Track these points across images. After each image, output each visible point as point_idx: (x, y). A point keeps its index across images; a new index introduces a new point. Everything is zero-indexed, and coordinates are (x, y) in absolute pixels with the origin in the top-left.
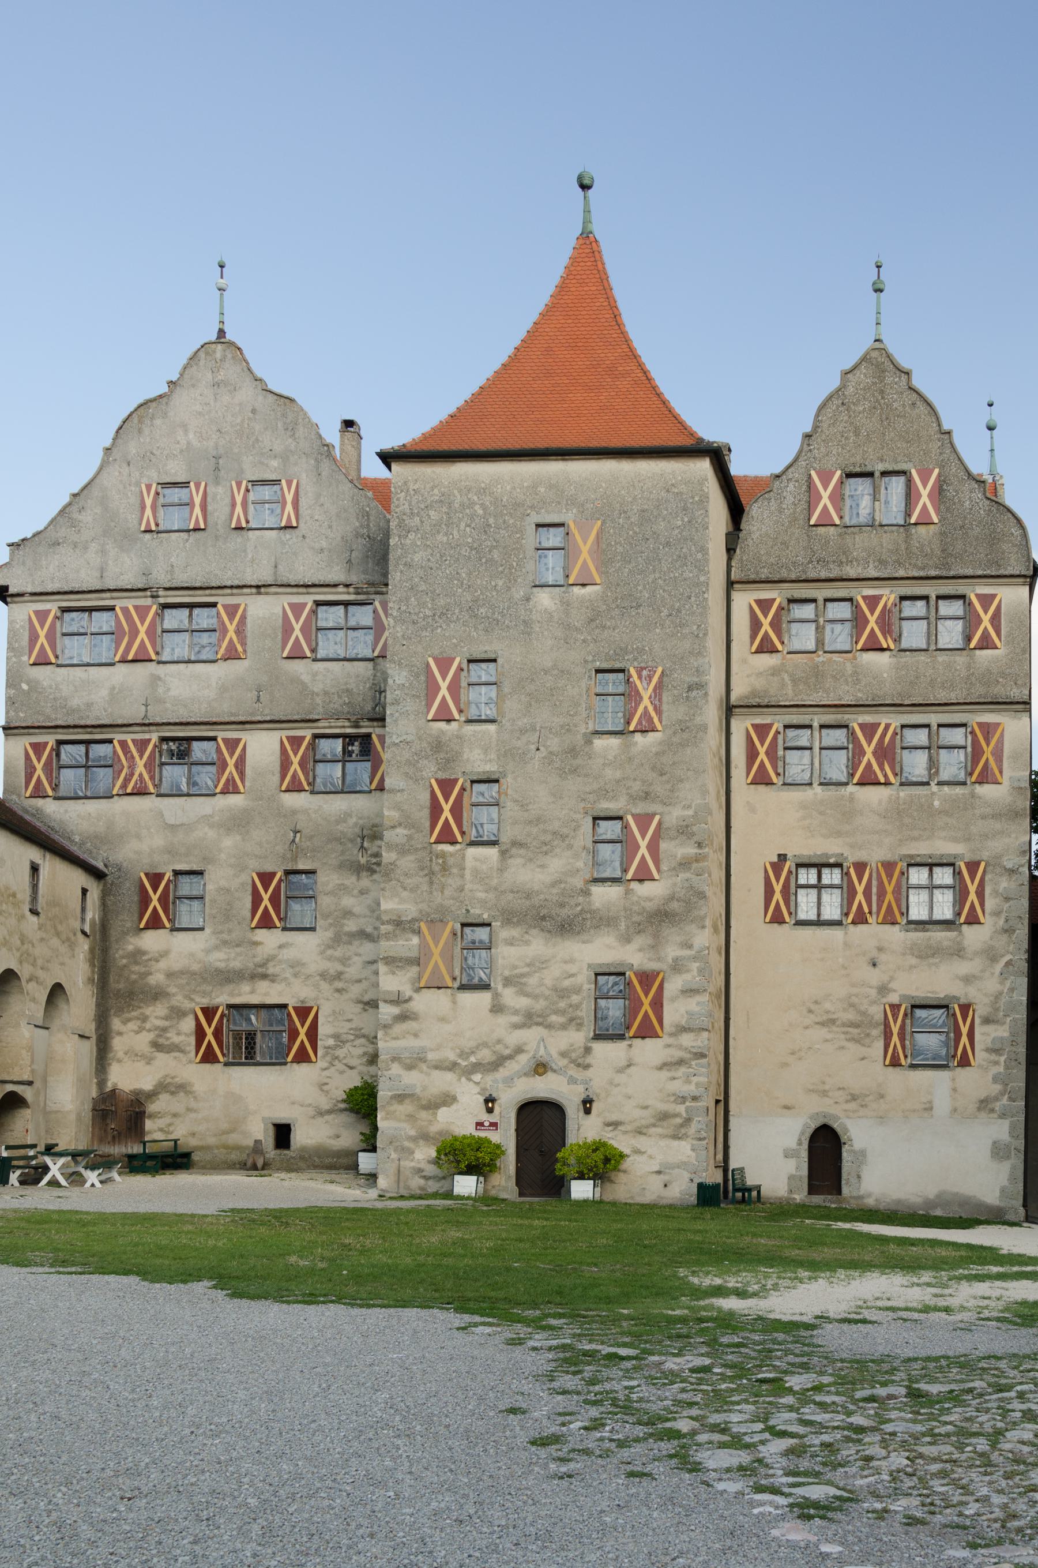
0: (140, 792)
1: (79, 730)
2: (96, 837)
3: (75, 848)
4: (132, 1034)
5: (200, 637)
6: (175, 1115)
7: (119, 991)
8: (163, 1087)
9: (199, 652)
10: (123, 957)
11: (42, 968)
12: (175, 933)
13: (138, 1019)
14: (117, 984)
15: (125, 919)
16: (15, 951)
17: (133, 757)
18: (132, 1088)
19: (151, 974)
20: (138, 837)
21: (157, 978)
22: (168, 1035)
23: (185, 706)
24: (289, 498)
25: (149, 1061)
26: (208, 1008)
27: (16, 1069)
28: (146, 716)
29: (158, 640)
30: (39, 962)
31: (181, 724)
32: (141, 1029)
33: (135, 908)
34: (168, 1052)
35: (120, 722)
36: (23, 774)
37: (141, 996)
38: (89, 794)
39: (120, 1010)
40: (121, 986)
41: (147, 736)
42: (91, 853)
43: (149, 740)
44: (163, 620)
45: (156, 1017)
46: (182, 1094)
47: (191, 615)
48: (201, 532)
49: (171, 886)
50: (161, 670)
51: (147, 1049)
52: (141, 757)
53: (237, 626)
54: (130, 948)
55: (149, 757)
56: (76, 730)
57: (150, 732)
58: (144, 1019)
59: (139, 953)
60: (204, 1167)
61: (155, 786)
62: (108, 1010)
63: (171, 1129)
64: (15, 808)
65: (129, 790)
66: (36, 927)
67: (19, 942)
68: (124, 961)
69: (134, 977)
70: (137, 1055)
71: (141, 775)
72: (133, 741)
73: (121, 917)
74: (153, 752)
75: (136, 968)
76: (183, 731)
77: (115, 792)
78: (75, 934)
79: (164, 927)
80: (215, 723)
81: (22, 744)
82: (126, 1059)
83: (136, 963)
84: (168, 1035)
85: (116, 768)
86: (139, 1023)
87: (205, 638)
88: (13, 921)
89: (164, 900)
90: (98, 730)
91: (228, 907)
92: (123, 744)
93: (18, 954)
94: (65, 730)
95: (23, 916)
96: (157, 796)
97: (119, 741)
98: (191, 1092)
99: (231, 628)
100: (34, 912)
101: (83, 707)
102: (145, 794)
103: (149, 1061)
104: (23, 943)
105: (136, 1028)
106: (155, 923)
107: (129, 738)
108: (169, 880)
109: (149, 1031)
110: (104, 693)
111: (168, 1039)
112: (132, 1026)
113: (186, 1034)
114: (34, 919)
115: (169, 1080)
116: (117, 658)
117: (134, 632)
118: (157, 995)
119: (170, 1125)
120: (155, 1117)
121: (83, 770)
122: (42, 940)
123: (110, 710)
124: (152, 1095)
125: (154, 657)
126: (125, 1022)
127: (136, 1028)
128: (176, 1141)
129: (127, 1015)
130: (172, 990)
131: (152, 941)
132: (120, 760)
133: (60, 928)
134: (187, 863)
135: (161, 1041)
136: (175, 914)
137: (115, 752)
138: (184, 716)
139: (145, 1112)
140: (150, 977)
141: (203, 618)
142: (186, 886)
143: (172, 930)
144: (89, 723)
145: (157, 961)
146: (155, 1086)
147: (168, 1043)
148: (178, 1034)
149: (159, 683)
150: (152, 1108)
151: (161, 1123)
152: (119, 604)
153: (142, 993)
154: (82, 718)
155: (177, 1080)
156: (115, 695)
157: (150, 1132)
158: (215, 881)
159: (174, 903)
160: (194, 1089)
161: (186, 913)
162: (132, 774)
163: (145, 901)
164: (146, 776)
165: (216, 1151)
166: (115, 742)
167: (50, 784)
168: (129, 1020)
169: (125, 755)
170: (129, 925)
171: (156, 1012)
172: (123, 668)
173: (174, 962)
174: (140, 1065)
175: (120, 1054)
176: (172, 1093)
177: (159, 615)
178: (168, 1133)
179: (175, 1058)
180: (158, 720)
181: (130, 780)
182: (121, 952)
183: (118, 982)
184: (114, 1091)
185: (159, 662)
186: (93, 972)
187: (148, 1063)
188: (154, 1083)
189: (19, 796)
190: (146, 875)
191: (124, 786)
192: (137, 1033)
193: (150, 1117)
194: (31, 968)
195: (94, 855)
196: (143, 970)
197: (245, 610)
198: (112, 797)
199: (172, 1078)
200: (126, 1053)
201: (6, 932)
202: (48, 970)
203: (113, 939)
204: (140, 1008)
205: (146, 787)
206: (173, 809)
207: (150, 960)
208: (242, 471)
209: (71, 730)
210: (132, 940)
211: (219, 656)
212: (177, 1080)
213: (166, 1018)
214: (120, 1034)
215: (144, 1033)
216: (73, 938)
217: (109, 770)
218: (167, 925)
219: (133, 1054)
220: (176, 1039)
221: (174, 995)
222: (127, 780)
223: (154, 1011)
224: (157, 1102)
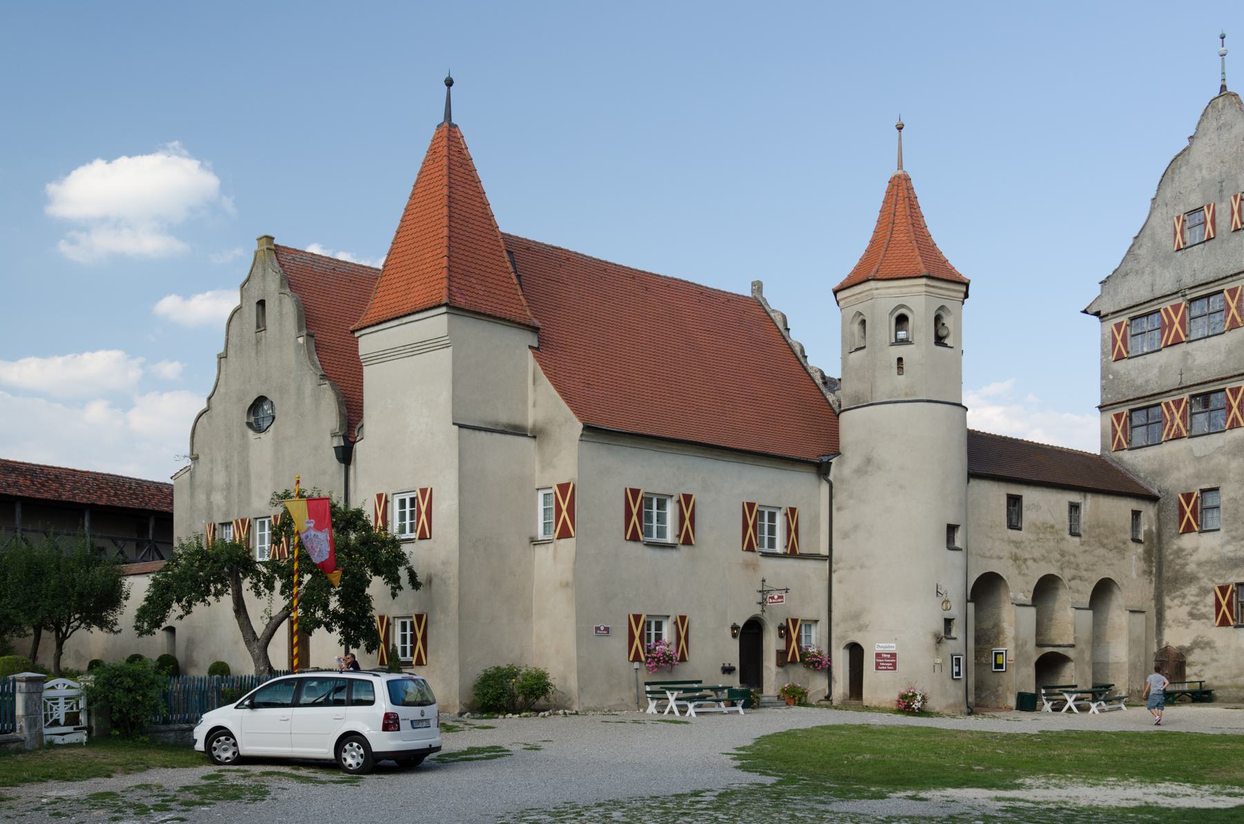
0: (1178, 437)
1: (1142, 400)
2: (1153, 472)
3: (1141, 482)
4: (1177, 607)
5: (1214, 317)
6: (1204, 664)
7: (1169, 578)
8: (1197, 644)
9: (1214, 328)
10: (1171, 554)
11: (1086, 570)
12: (1202, 534)
13: (1180, 596)
14: (1168, 574)
15: (1172, 527)
16: (1054, 563)
17: (1173, 413)
18: (1177, 645)
19: (1187, 564)
20: (1178, 469)
21: (1191, 568)
22: (1199, 607)
23: (1205, 370)
24: (1209, 218)
25: (1187, 626)
26: (1222, 587)
27: (1066, 637)
28: (1181, 382)
29: (1187, 325)
30: (1083, 566)
31: (1201, 384)
32: (1182, 604)
33: (1177, 519)
34: (1199, 619)
35: (1165, 390)
36: (1111, 436)
37: (1182, 581)
38: (1149, 443)
39: (1170, 591)
40: (1170, 574)
41: (1182, 396)
42: (1151, 484)
43: (1183, 399)
44: (1190, 311)
45: (1192, 595)
46: (1208, 649)
47: (1209, 302)
48: (1212, 240)
49: (1199, 501)
50: (1189, 347)
51: (1186, 618)
52: (1178, 412)
53: (1237, 303)
54: (1175, 547)
55: (1183, 411)
56: (1139, 401)
57: (1183, 393)
58: (1184, 597)
59: (1181, 550)
60: (1223, 701)
61: (1187, 431)
62: (1163, 592)
63: (1202, 673)
64: (1107, 459)
65: (1171, 437)
66: (1079, 543)
67: (1059, 557)
68: (1172, 557)
69: (1177, 567)
70: (1180, 622)
71: (1178, 425)
72: (1173, 401)
73: (1169, 527)
74: (1186, 406)
75: (1178, 561)
76: (1203, 388)
77: (1163, 440)
78: (1125, 543)
79: (1195, 531)
80: (1222, 379)
81: (1110, 415)
82: (1173, 625)
83: (1179, 558)
84: (1199, 607)
85: (1164, 422)
86: (1181, 600)
87: (1218, 317)
88: (1052, 544)
89: (1194, 512)
90: (1152, 398)
91: (1235, 512)
92: (1167, 405)
93: (1059, 564)
94: (1133, 402)
95: (1063, 539)
96: (1189, 438)
97: (1165, 403)
98: (1214, 648)
99: (1233, 305)
100: (1074, 534)
101: (1143, 384)
102: (1181, 438)
103: (1187, 626)
104: (1063, 556)
105: (1179, 603)
106: (1189, 529)
107: (1170, 400)
108: (1197, 497)
109: (1187, 605)
110: (1156, 371)
111: (1198, 610)
112: (1177, 602)
113: (1210, 606)
114: (1077, 539)
115: (1200, 639)
116: (1162, 346)
117: (1172, 323)
118: (1192, 579)
119: (1201, 671)
120: (1192, 665)
121: (1145, 427)
122: (1085, 551)
123: (1159, 382)
124: (1189, 650)
125: (1184, 339)
126: (1172, 600)
127: (1179, 603)
128: (1201, 682)
129: (1173, 595)
130: (1201, 575)
131: (1188, 541)
132: (1165, 416)
133: (1105, 541)
134: (1208, 483)
135: (1195, 611)
136: (1202, 521)
137: (1163, 411)
138: (1205, 376)
139: (1185, 662)
140: (1187, 567)
141: (1216, 303)
142: (1210, 500)
143: (1200, 532)
144: (1148, 394)
145: (1191, 555)
146: (1191, 643)
147: (1198, 613)
148: (1205, 606)
149: (1189, 357)
150: (1190, 659)
151: (1195, 669)
152: (1162, 306)
153: (1183, 578)
154: (1143, 391)
155: (1205, 638)
156: (1162, 371)
157: (1189, 676)
158: (1224, 498)
159: (1201, 513)
160: (1215, 645)
161: (1212, 520)
162: (1172, 426)
163: (1182, 513)
164: (1181, 425)
165: (1230, 690)
166: (1227, 390)
167: (1126, 440)
168: (1175, 598)
169: (1168, 412)
170: (1174, 531)
171: (1191, 591)
172: (1166, 351)
173: (1201, 556)
174: (1182, 629)
175: (1170, 622)
176: (1202, 648)
177: (1188, 308)
178: (1201, 676)
179: (1203, 623)
180: (1189, 383)
181: (1171, 430)
182: (1169, 551)
183: (1168, 572)
184: (1166, 647)
185: (1188, 342)
186: (1150, 567)
187: (1187, 628)
188: (1191, 641)
189: (1109, 451)
190: (1183, 495)
191: (1168, 435)
192: (1180, 606)
193: (1189, 665)
194: (1073, 572)
195: (1152, 485)
196: (1183, 562)
197: (1242, 290)
198: (1161, 443)
199: (1202, 637)
200: (1173, 621)
201: (1044, 552)
202: (1094, 570)
203: (1164, 542)
204: (1181, 589)
205: (1181, 433)
206: (1199, 446)
207: (1187, 555)
208: (1238, 187)
209: (1136, 401)
210: (1176, 542)
211: (1225, 329)
212: (1205, 638)
213: (1197, 595)
214: (1170, 608)
215: (1184, 606)
216: (1122, 546)
217: (1160, 424)
218: (1196, 529)
219: (1178, 621)
220: (1204, 610)
221: (1202, 578)
222: (1170, 430)
223: (1190, 591)
224: (1193, 655)
